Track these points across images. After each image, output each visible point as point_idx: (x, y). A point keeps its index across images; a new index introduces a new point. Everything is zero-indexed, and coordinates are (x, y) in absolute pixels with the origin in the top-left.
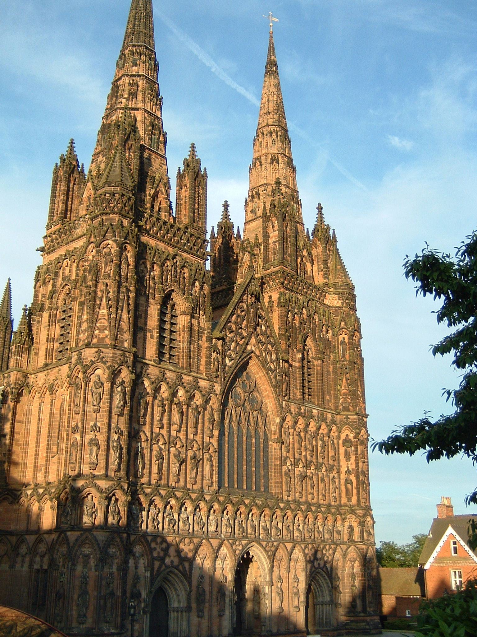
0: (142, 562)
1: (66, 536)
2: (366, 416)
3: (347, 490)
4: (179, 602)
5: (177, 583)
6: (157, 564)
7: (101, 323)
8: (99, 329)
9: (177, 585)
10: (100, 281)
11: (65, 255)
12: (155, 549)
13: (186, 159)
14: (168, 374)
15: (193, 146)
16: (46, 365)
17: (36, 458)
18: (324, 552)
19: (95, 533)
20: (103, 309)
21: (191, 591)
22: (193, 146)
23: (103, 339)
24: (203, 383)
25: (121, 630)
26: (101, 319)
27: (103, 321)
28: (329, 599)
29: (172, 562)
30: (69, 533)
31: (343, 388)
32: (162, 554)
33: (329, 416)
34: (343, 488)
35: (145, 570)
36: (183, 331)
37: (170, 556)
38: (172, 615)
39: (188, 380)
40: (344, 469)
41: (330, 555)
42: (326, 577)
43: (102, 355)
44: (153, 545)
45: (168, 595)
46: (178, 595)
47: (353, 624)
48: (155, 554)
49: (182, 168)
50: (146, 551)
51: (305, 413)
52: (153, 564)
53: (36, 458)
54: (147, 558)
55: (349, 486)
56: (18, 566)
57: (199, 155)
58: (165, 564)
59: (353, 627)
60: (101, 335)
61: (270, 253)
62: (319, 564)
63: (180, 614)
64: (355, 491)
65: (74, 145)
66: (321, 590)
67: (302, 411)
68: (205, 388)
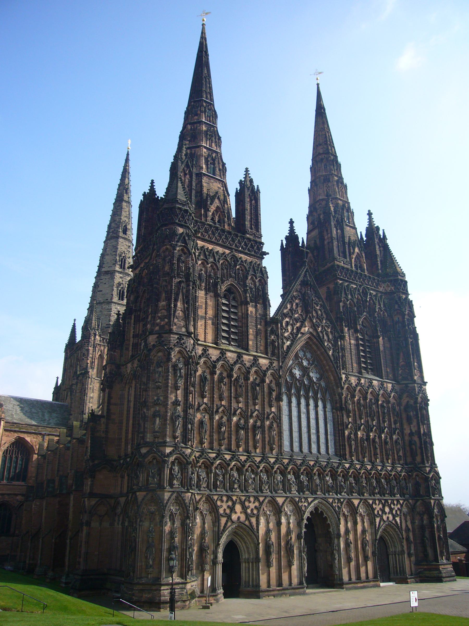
0: (208, 519)
1: (136, 496)
2: (425, 383)
3: (411, 450)
4: (249, 553)
5: (246, 537)
6: (223, 520)
7: (162, 313)
8: (159, 318)
9: (246, 539)
10: (161, 279)
11: (144, 266)
12: (221, 506)
13: (241, 180)
14: (229, 354)
15: (247, 170)
16: (132, 356)
17: (127, 433)
18: (392, 506)
19: (158, 493)
20: (164, 301)
21: (259, 544)
22: (247, 170)
23: (163, 326)
24: (263, 362)
25: (186, 580)
26: (161, 310)
27: (163, 311)
28: (400, 549)
29: (239, 518)
30: (138, 493)
31: (401, 361)
32: (228, 511)
33: (390, 386)
34: (408, 448)
35: (213, 525)
36: (243, 318)
37: (236, 513)
38: (243, 565)
39: (249, 359)
40: (407, 431)
41: (398, 509)
42: (397, 530)
43: (163, 339)
44: (219, 503)
45: (240, 547)
46: (248, 548)
47: (427, 572)
48: (221, 511)
49: (239, 188)
50: (213, 508)
51: (365, 384)
52: (219, 520)
53: (127, 433)
54: (215, 515)
55: (414, 447)
56: (116, 523)
57: (252, 175)
58: (231, 519)
59: (427, 575)
60: (162, 323)
61: (326, 252)
62: (388, 518)
63: (251, 564)
64: (419, 451)
65: (154, 184)
66: (392, 541)
67: (363, 381)
68: (265, 365)
